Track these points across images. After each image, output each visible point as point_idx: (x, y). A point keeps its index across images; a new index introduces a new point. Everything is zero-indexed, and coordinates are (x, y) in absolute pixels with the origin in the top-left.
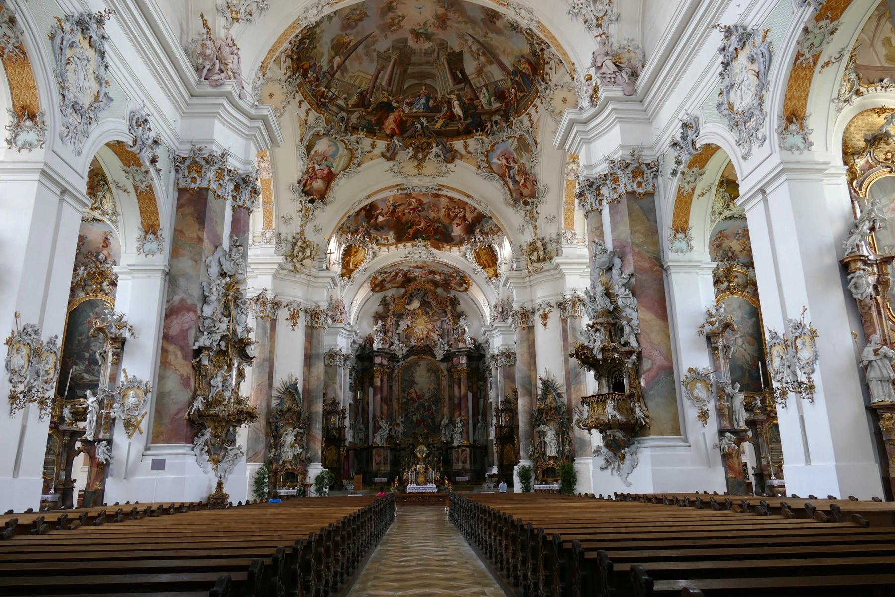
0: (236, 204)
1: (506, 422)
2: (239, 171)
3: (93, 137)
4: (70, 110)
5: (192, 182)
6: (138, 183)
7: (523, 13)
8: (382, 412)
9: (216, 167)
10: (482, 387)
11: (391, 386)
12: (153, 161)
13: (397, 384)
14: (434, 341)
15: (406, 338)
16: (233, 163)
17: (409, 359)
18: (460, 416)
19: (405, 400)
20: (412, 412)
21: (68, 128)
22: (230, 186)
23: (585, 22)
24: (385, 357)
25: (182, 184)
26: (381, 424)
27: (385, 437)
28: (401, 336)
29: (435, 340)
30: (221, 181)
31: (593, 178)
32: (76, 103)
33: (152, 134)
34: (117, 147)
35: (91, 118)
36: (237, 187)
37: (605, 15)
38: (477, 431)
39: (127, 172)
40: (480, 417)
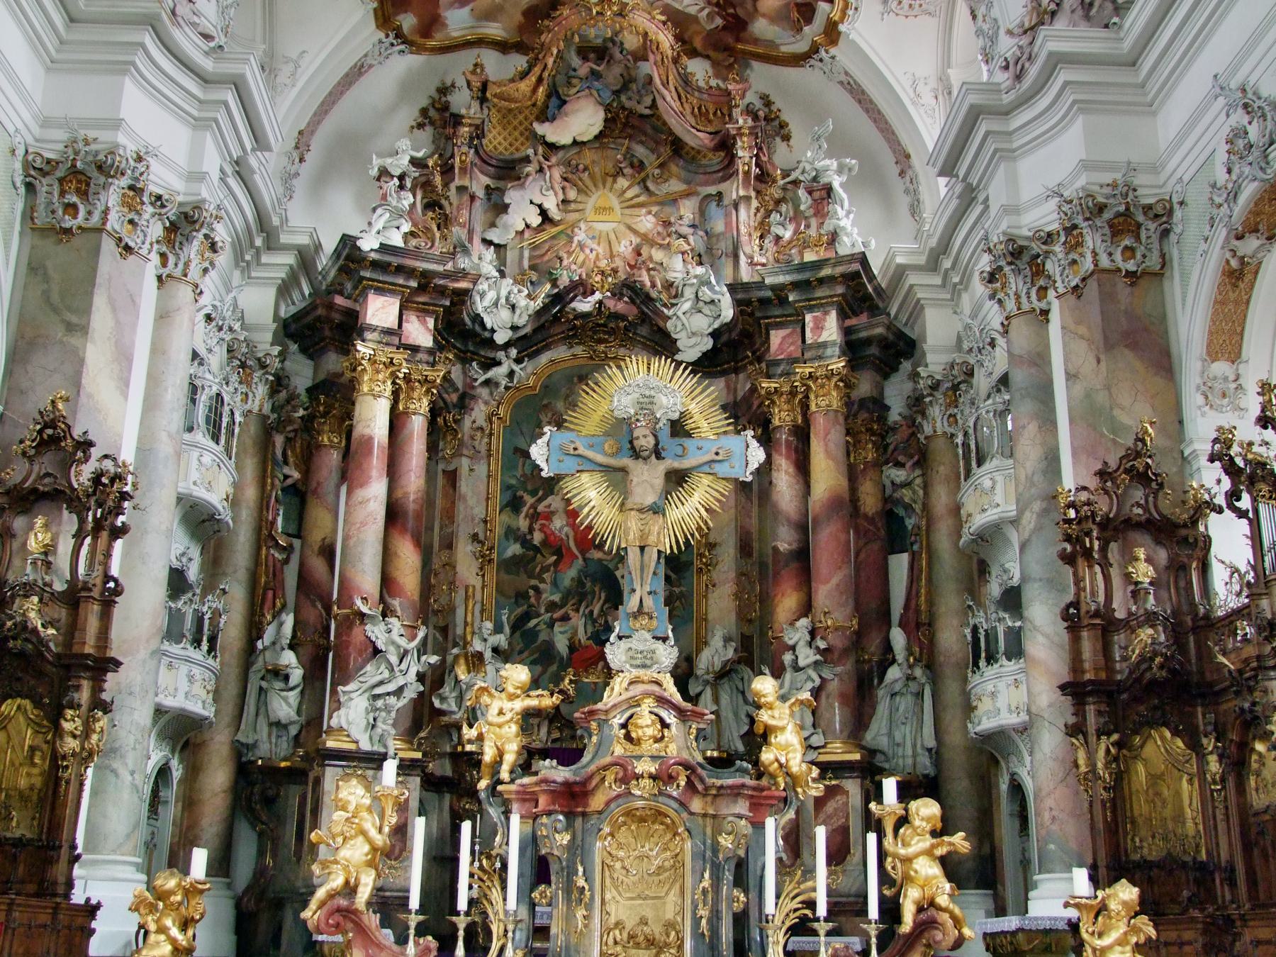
1: (1137, 593)
8: (387, 582)
10: (906, 495)
11: (452, 477)
13: (482, 469)
14: (669, 285)
15: (532, 267)
17: (544, 358)
18: (807, 608)
19: (514, 549)
20: (552, 606)
24: (423, 311)
26: (376, 632)
27: (396, 703)
28: (511, 256)
29: (671, 276)
38: (883, 708)
40: (898, 638)
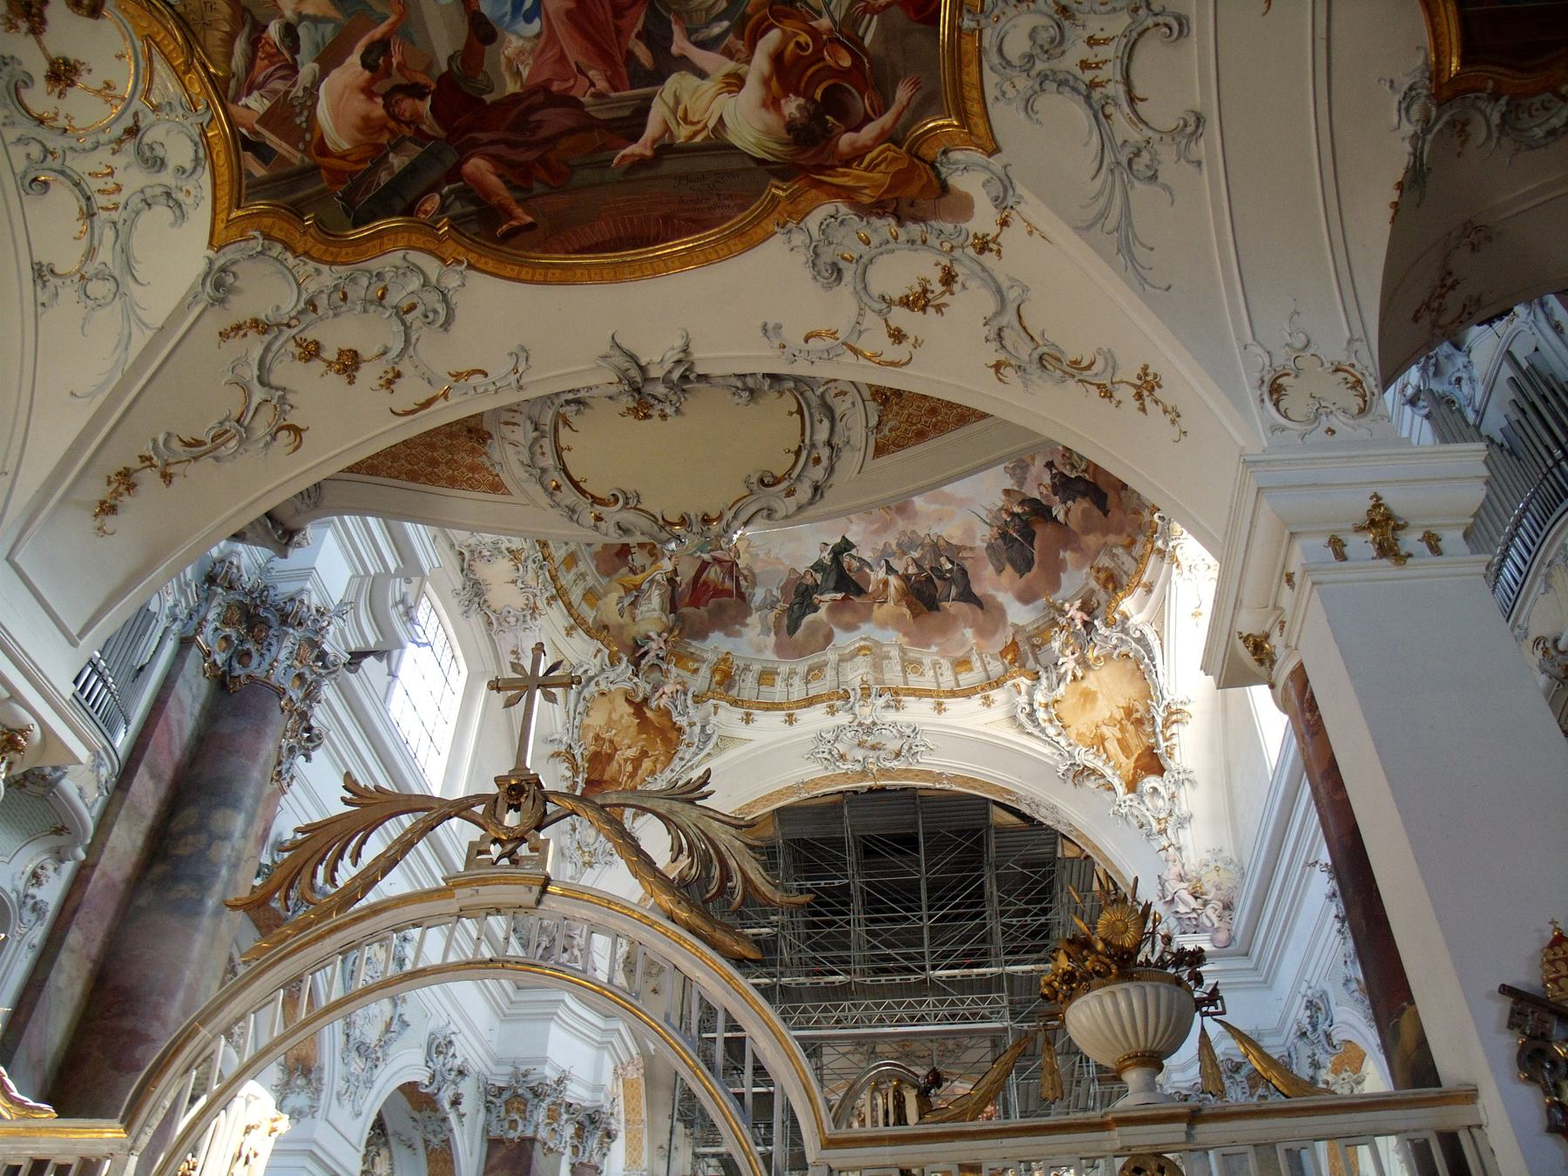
0: (576, 1161)
2: (587, 1104)
3: (377, 1085)
4: (354, 1054)
5: (510, 1128)
6: (431, 1137)
7: (1043, 811)
9: (548, 1100)
12: (455, 1103)
16: (576, 1093)
21: (348, 1081)
22: (570, 1130)
23: (1141, 826)
25: (496, 1132)
30: (555, 1125)
31: (1187, 1089)
32: (363, 1043)
33: (458, 1061)
34: (409, 1090)
35: (378, 1059)
36: (580, 1132)
37: (1170, 815)
39: (414, 1120)
